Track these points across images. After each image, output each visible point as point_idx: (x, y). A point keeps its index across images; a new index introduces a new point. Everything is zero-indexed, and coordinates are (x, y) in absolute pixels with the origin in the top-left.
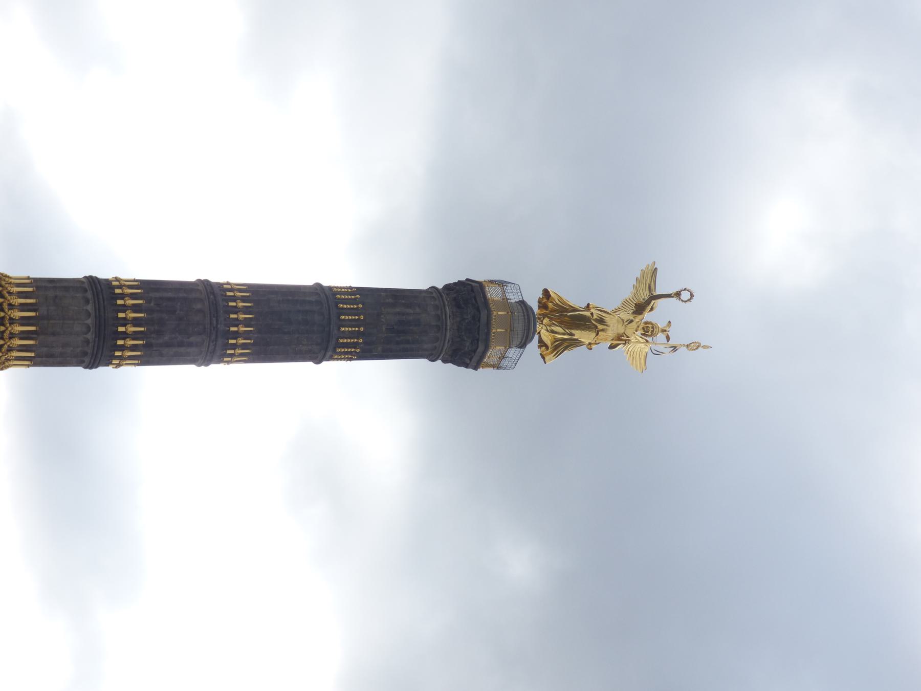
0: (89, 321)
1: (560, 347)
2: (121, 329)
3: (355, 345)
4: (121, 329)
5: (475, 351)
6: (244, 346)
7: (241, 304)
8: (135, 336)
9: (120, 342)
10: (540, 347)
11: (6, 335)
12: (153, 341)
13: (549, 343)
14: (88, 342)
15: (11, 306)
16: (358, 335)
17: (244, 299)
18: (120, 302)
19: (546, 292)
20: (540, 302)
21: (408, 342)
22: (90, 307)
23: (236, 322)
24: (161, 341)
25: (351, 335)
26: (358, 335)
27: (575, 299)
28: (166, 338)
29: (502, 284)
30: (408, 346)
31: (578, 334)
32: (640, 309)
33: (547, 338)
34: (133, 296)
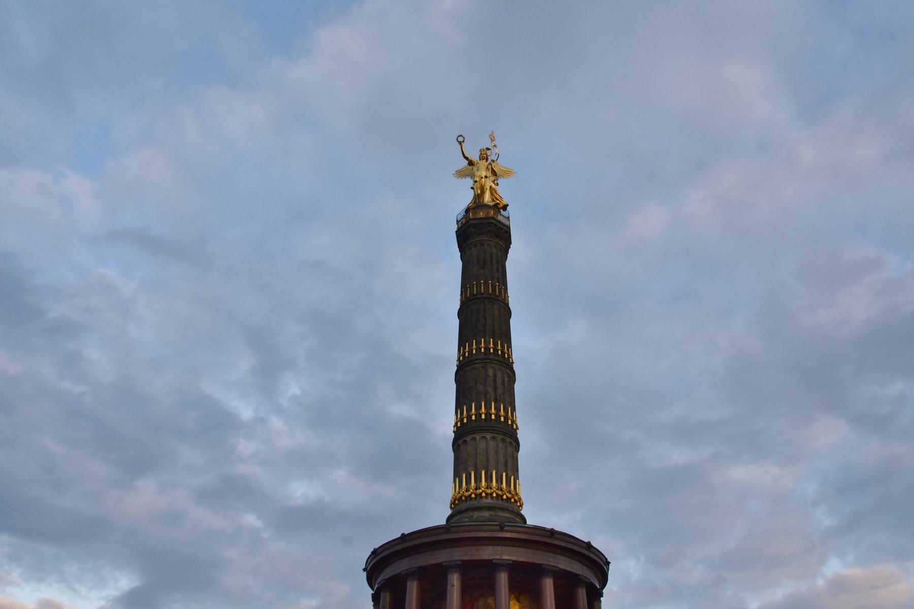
0: (478, 437)
2: (483, 416)
4: (483, 416)
5: (496, 225)
8: (488, 408)
9: (493, 417)
11: (489, 491)
12: (493, 397)
15: (467, 490)
16: (486, 283)
17: (464, 349)
18: (465, 421)
21: (491, 260)
22: (468, 439)
24: (492, 394)
26: (486, 283)
28: (490, 390)
30: (494, 261)
34: (462, 413)
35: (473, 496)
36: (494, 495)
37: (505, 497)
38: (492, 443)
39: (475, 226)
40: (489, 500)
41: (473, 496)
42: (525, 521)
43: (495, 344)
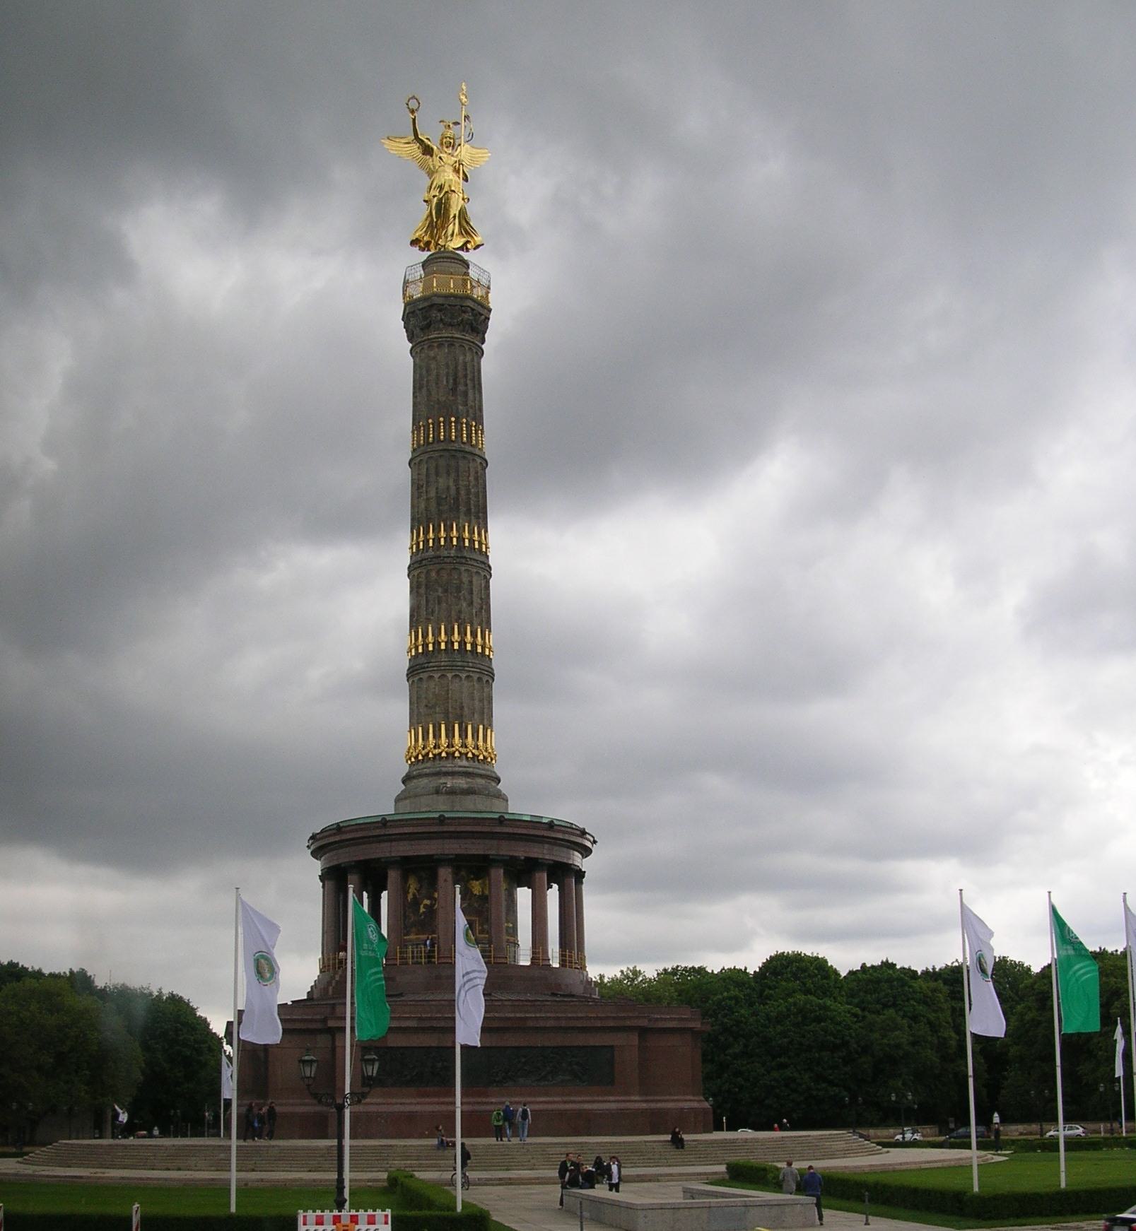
0: (450, 675)
1: (466, 229)
2: (456, 646)
3: (469, 426)
4: (456, 646)
6: (471, 532)
7: (431, 535)
9: (469, 647)
10: (468, 250)
13: (464, 240)
14: (468, 677)
19: (414, 242)
20: (423, 250)
21: (465, 376)
22: (436, 676)
23: (449, 539)
25: (459, 431)
27: (421, 213)
29: (406, 283)
31: (454, 211)
32: (428, 151)
33: (457, 242)
34: (425, 636)
35: (444, 754)
36: (470, 755)
37: (481, 757)
38: (465, 683)
39: (440, 308)
40: (464, 763)
41: (444, 754)
42: (498, 780)
43: (471, 532)
